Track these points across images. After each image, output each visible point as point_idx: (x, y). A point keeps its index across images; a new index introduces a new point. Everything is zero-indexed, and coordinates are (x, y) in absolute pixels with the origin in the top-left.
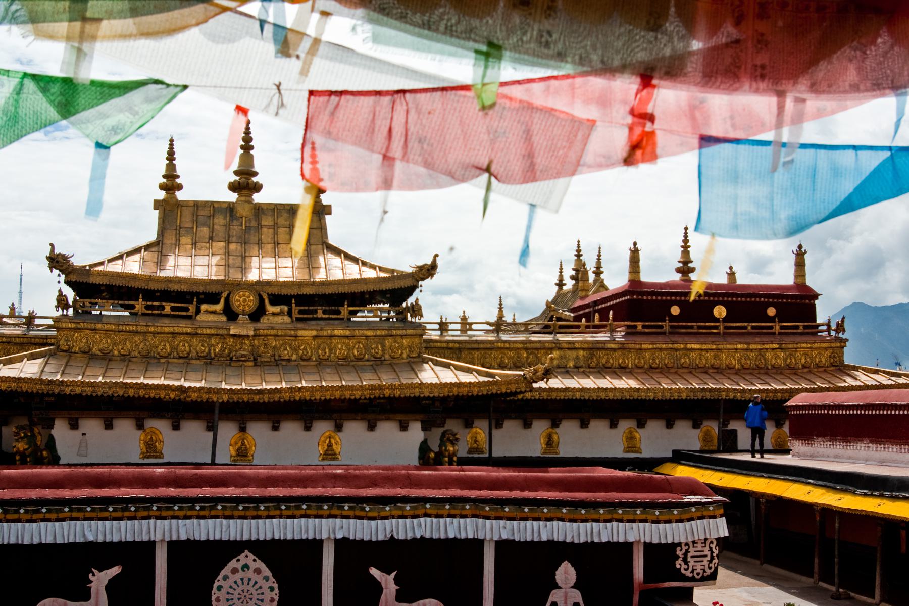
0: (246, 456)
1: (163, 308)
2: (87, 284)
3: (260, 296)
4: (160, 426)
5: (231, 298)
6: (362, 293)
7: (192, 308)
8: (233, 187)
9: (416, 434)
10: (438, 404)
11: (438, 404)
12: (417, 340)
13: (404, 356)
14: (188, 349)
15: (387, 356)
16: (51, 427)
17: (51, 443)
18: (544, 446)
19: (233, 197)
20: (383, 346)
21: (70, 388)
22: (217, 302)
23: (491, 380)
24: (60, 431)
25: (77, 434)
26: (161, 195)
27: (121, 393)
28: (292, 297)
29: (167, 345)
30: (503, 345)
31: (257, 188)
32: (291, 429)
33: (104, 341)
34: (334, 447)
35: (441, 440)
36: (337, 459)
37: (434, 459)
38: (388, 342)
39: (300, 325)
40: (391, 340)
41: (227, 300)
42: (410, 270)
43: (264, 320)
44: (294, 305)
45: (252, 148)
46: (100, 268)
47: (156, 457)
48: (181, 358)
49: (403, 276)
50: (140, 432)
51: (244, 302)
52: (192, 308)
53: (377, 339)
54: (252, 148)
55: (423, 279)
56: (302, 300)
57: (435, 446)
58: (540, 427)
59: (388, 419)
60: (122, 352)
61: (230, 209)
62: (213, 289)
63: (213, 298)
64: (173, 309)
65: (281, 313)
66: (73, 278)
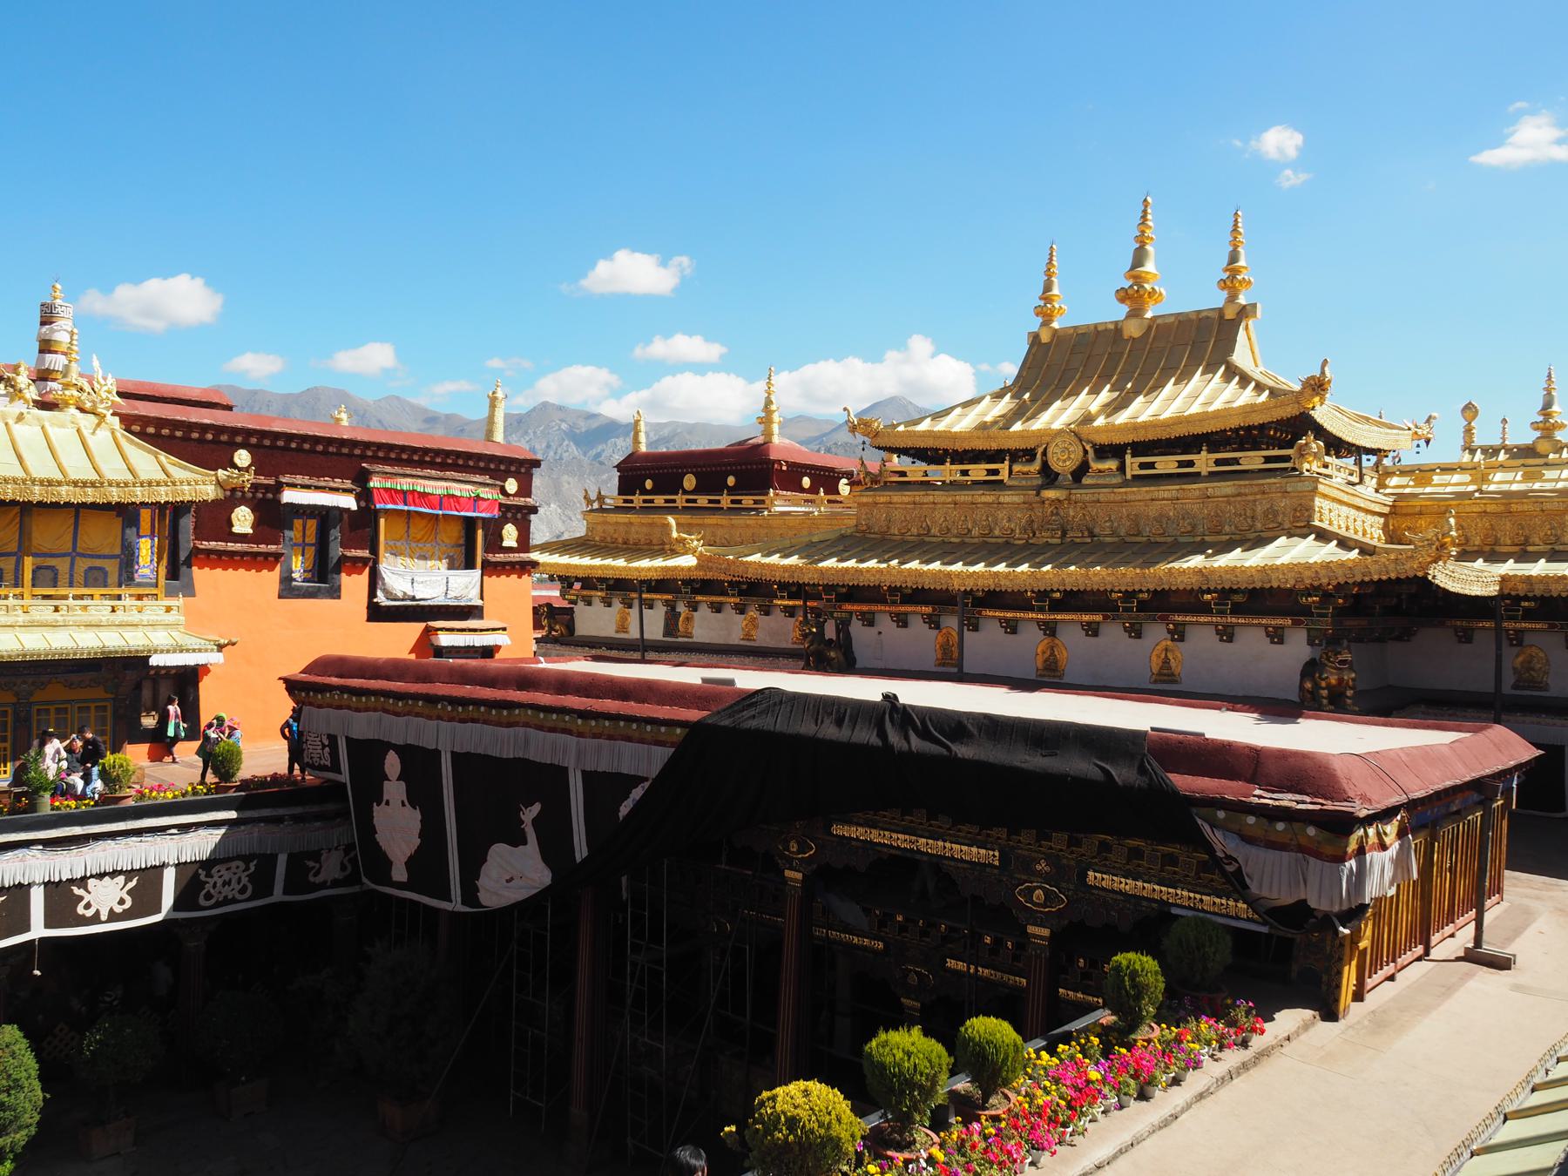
0: (1055, 670)
28: (1126, 446)
34: (1173, 663)
36: (1175, 682)
41: (1044, 453)
43: (1086, 481)
50: (935, 632)
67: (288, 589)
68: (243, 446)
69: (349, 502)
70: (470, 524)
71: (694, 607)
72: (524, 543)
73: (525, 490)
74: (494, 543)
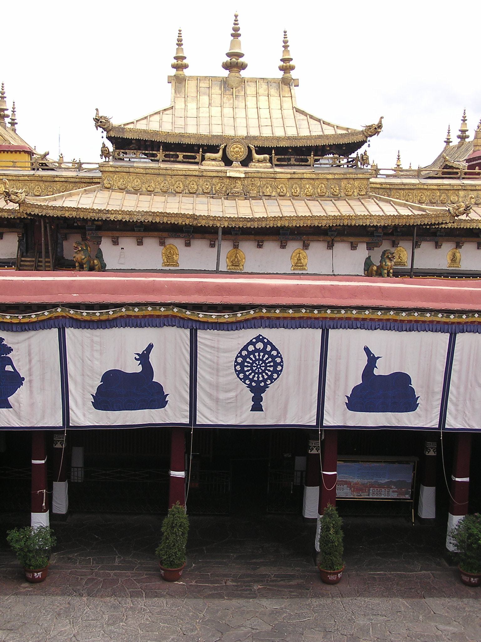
1: (178, 156)
2: (123, 139)
3: (249, 147)
4: (178, 244)
5: (227, 150)
6: (324, 146)
7: (199, 157)
8: (226, 66)
9: (362, 252)
10: (380, 230)
11: (380, 230)
12: (365, 182)
13: (356, 194)
14: (196, 187)
15: (343, 194)
16: (99, 243)
17: (99, 255)
18: (450, 261)
20: (340, 186)
21: (114, 216)
22: (217, 152)
23: (424, 213)
24: (106, 246)
25: (118, 248)
26: (173, 72)
27: (150, 220)
28: (272, 148)
29: (181, 183)
30: (422, 187)
31: (243, 67)
32: (271, 247)
33: (135, 181)
35: (382, 257)
37: (376, 271)
38: (343, 183)
39: (278, 170)
40: (345, 182)
41: (224, 150)
42: (361, 129)
44: (273, 155)
45: (239, 35)
46: (131, 126)
47: (174, 265)
48: (191, 193)
49: (355, 133)
50: (163, 247)
51: (237, 151)
52: (199, 157)
53: (335, 181)
54: (239, 35)
55: (371, 136)
56: (280, 151)
57: (376, 261)
58: (447, 248)
59: (343, 241)
60: (149, 189)
62: (214, 143)
63: (214, 149)
64: (184, 157)
65: (264, 161)
66: (112, 134)
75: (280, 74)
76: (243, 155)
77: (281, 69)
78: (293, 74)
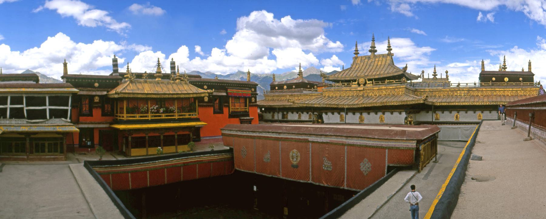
8: (370, 51)
9: (404, 115)
19: (370, 54)
31: (376, 51)
32: (372, 114)
38: (396, 90)
51: (362, 80)
56: (376, 79)
58: (454, 113)
61: (369, 58)
62: (355, 79)
63: (355, 81)
67: (215, 112)
68: (206, 85)
69: (224, 94)
70: (245, 98)
71: (287, 113)
72: (256, 101)
73: (255, 90)
74: (250, 101)
75: (387, 52)
76: (364, 83)
77: (387, 50)
78: (392, 52)
